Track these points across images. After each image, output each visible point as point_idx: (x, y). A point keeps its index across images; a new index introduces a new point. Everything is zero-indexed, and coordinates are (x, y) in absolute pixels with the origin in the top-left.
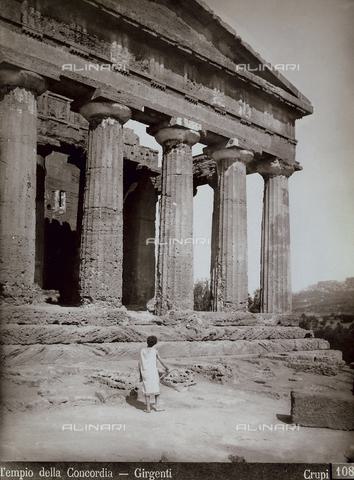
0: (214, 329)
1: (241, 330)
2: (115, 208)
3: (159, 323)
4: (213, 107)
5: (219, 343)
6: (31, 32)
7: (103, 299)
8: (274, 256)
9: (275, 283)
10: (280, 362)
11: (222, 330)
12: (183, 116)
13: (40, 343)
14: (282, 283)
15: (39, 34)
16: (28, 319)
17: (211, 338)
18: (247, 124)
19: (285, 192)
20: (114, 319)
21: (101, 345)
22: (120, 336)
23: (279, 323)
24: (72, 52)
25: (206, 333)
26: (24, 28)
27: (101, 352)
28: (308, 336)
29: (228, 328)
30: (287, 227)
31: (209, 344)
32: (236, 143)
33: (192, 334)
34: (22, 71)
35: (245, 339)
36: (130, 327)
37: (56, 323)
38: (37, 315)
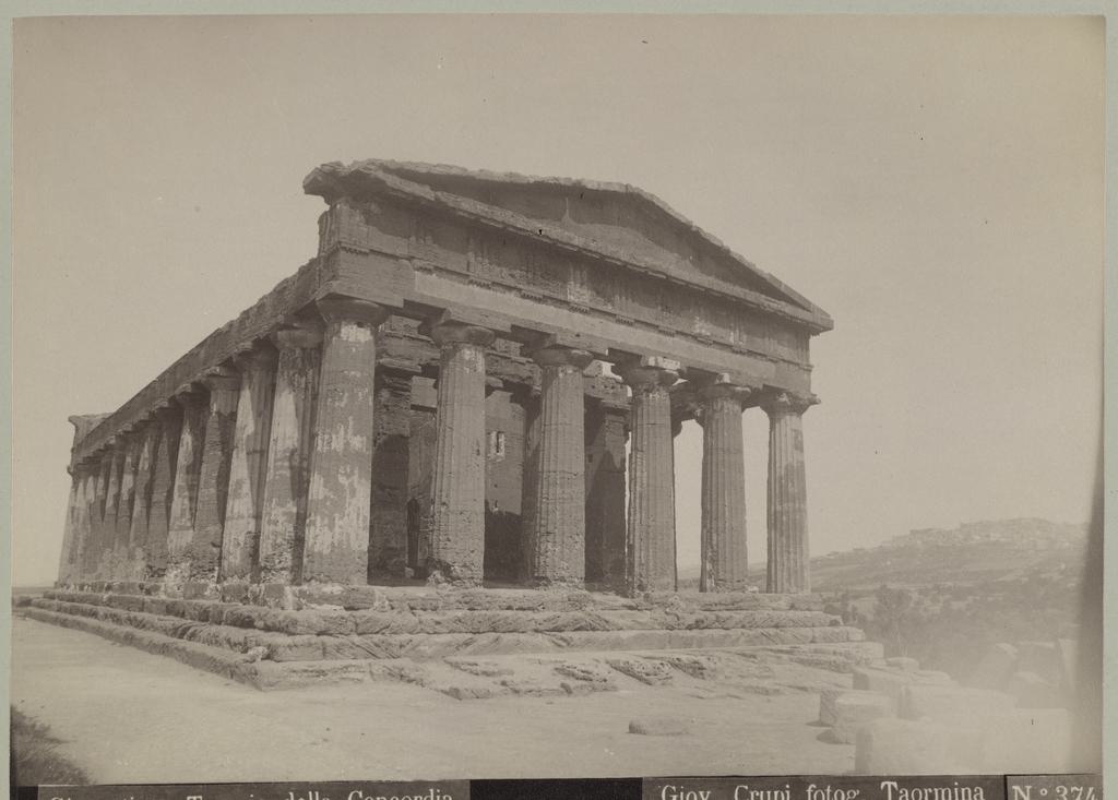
0: (701, 615)
1: (738, 616)
2: (574, 471)
3: (631, 608)
5: (707, 632)
6: (478, 280)
7: (563, 579)
8: (784, 518)
9: (785, 554)
11: (711, 616)
12: (657, 354)
13: (494, 631)
14: (795, 553)
17: (698, 625)
18: (741, 353)
19: (798, 433)
20: (576, 603)
21: (563, 634)
22: (583, 624)
23: (792, 607)
24: (524, 297)
25: (691, 620)
29: (720, 614)
31: (695, 633)
32: (727, 379)
33: (670, 620)
34: (470, 328)
35: (743, 627)
36: (597, 613)
37: (509, 608)
38: (489, 599)
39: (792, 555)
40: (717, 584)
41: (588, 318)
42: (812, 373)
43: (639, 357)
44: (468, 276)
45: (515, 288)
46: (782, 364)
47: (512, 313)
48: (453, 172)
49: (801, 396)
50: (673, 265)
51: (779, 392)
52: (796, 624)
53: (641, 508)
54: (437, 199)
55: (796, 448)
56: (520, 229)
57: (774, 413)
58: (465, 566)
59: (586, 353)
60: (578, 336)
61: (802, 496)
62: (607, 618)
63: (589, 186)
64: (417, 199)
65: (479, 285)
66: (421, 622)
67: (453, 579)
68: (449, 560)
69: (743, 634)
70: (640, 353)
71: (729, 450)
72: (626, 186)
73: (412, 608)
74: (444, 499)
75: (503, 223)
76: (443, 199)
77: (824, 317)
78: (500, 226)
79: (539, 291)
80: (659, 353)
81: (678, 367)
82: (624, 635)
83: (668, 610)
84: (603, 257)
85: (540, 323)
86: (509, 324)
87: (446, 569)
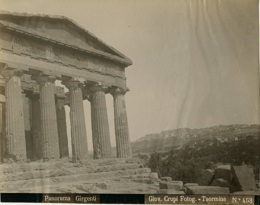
1: (110, 167)
2: (54, 119)
3: (76, 166)
4: (88, 70)
5: (102, 173)
6: (16, 53)
7: (53, 158)
10: (130, 180)
15: (19, 53)
16: (27, 169)
17: (98, 171)
18: (104, 74)
19: (123, 102)
20: (58, 166)
23: (127, 162)
24: (32, 58)
26: (14, 52)
27: (55, 180)
28: (141, 167)
29: (105, 166)
30: (126, 118)
31: (97, 174)
32: (100, 84)
33: (89, 169)
34: (15, 70)
35: (112, 170)
39: (125, 144)
40: (102, 156)
41: (53, 64)
42: (126, 80)
43: (71, 78)
44: (13, 51)
45: (29, 55)
46: (117, 78)
49: (124, 88)
51: (116, 87)
52: (129, 168)
53: (75, 131)
55: (123, 107)
57: (114, 95)
58: (21, 156)
59: (54, 77)
60: (51, 71)
61: (126, 124)
62: (69, 171)
63: (51, 17)
65: (17, 54)
66: (8, 177)
67: (17, 161)
68: (15, 154)
69: (113, 173)
70: (71, 76)
73: (4, 172)
74: (11, 132)
77: (130, 61)
78: (23, 32)
81: (84, 80)
82: (75, 176)
83: (88, 166)
84: (57, 42)
85: (38, 67)
86: (28, 68)
87: (14, 158)
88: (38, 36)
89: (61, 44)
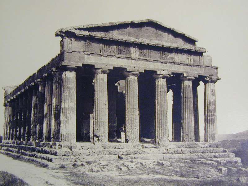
11: (179, 150)
18: (191, 66)
23: (210, 146)
25: (172, 151)
29: (182, 149)
33: (166, 151)
35: (190, 153)
37: (115, 148)
38: (109, 146)
42: (218, 69)
47: (113, 63)
48: (93, 26)
50: (167, 41)
51: (206, 77)
54: (90, 35)
55: (212, 95)
56: (115, 39)
57: (206, 82)
60: (135, 67)
61: (215, 110)
63: (136, 22)
64: (84, 36)
71: (187, 97)
72: (148, 20)
75: (109, 38)
76: (91, 35)
78: (109, 39)
79: (122, 56)
80: (161, 70)
84: (141, 43)
88: (123, 40)
89: (144, 44)
